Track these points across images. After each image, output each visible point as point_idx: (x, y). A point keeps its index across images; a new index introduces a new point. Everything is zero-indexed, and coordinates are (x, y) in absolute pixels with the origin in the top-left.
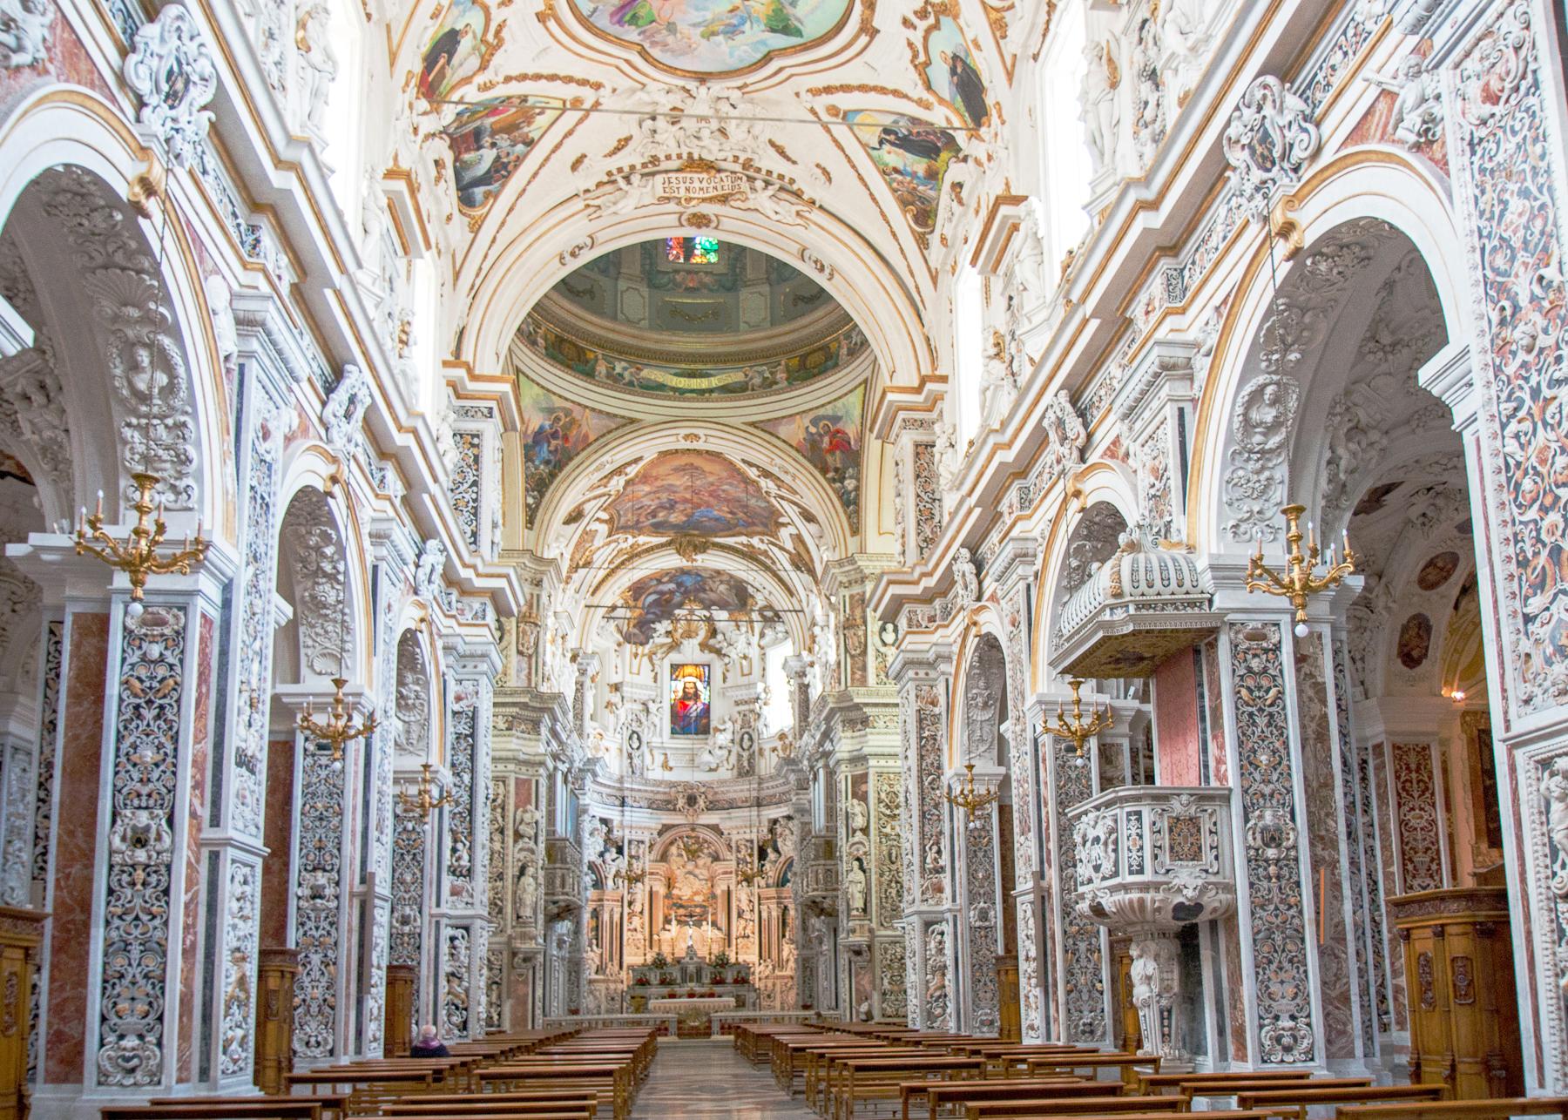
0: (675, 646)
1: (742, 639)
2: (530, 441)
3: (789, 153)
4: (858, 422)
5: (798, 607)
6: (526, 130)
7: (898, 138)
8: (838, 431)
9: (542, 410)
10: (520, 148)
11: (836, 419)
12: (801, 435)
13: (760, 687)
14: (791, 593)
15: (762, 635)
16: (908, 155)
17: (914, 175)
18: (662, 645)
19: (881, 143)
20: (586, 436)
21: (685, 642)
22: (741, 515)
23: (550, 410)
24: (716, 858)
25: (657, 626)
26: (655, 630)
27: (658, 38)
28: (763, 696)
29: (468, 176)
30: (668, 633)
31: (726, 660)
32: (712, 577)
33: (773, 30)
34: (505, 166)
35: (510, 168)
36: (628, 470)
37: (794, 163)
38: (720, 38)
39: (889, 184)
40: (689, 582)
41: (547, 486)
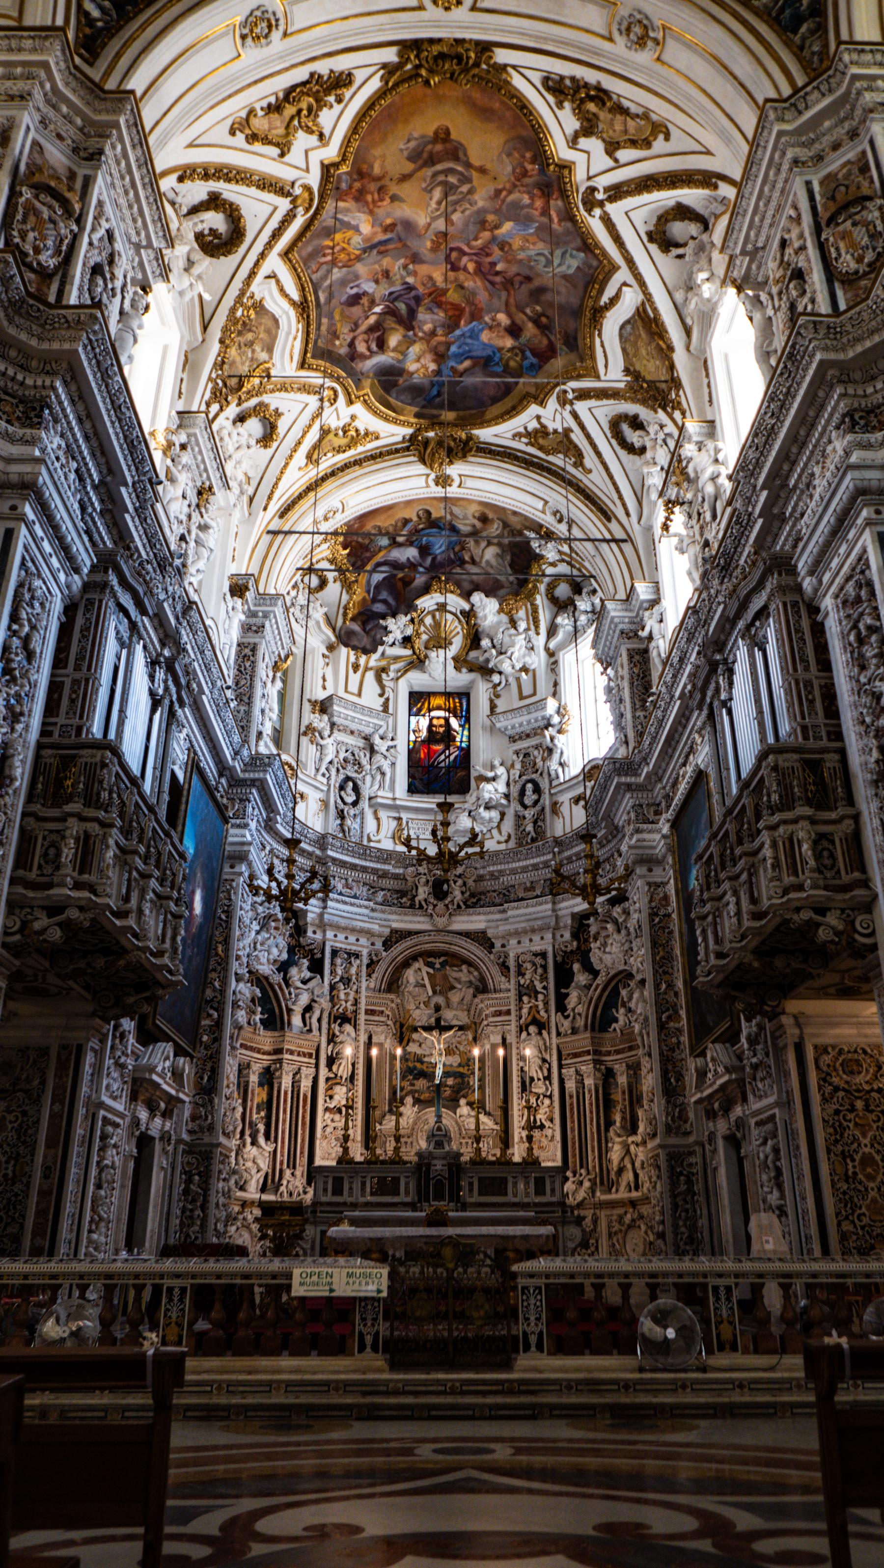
0: (418, 663)
1: (520, 641)
5: (620, 534)
13: (551, 705)
14: (606, 515)
15: (552, 631)
18: (396, 659)
21: (433, 654)
22: (530, 330)
24: (482, 988)
25: (390, 623)
26: (386, 631)
28: (556, 720)
30: (407, 641)
31: (496, 678)
32: (475, 533)
36: (326, 118)
40: (439, 545)
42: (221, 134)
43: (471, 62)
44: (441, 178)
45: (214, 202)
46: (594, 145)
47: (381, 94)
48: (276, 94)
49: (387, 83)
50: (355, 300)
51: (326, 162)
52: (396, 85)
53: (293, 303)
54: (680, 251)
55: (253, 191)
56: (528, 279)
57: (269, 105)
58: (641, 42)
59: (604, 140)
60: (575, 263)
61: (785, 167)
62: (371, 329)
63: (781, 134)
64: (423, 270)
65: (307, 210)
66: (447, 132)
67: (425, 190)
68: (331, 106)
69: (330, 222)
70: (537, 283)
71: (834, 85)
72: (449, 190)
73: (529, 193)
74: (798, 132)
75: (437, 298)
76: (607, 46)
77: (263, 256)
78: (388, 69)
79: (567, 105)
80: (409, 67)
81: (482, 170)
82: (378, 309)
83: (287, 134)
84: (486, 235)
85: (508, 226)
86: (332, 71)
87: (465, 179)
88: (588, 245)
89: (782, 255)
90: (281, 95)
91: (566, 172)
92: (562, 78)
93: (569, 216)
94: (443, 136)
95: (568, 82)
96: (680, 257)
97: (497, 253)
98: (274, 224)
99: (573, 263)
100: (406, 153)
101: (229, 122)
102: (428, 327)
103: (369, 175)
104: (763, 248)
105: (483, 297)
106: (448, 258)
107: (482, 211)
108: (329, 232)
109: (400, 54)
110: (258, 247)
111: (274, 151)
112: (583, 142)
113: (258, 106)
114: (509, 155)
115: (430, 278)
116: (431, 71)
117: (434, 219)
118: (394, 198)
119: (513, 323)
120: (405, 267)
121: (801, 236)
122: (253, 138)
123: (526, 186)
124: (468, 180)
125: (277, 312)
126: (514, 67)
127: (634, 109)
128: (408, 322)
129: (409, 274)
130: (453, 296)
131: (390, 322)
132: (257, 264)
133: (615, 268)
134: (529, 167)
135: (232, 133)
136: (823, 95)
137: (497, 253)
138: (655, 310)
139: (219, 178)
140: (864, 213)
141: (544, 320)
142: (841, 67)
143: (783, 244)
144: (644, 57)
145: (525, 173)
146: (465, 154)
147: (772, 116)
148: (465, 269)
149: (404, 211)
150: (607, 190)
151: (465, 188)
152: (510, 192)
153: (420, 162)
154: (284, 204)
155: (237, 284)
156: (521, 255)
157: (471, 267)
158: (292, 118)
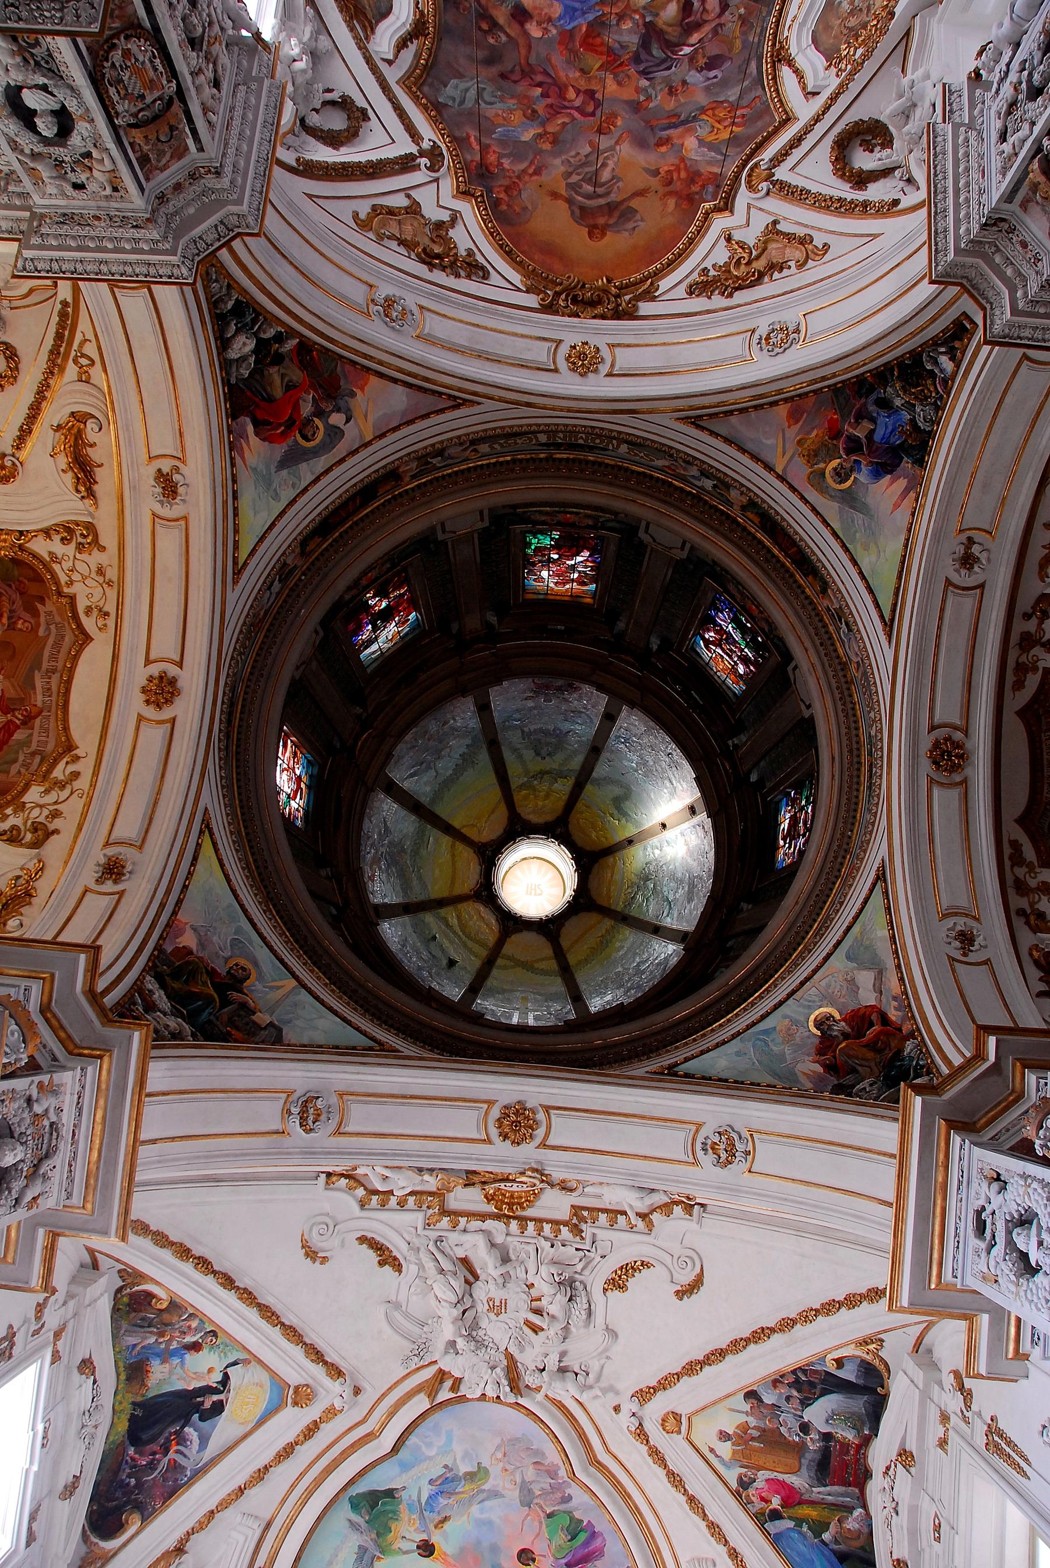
2: (907, 464)
3: (372, 1256)
4: (243, 475)
6: (752, 1421)
7: (197, 1408)
8: (284, 436)
9: (863, 508)
10: (769, 1398)
11: (291, 460)
12: (360, 401)
16: (179, 1386)
17: (165, 1356)
19: (226, 1379)
20: (794, 416)
23: (850, 499)
27: (546, 1482)
29: (858, 1404)
33: (390, 1493)
34: (797, 1384)
35: (791, 1379)
36: (721, 255)
37: (362, 1240)
38: (463, 1468)
39: (203, 1318)
41: (900, 361)
42: (838, 246)
43: (563, 296)
44: (600, 191)
45: (861, 180)
46: (432, 213)
47: (659, 274)
48: (771, 280)
49: (652, 284)
50: (713, 63)
51: (727, 213)
52: (643, 281)
53: (790, 63)
54: (329, 96)
55: (814, 188)
56: (503, 76)
57: (781, 270)
58: (389, 303)
59: (423, 217)
60: (449, 90)
61: (228, 170)
62: (698, 26)
63: (239, 202)
64: (627, 94)
65: (756, 165)
66: (591, 235)
67: (619, 180)
68: (714, 266)
69: (731, 151)
70: (494, 70)
71: (191, 246)
72: (594, 179)
73: (503, 169)
74: (222, 204)
75: (613, 62)
76: (425, 303)
77: (817, 119)
78: (650, 296)
79: (464, 254)
80: (627, 297)
81: (555, 195)
82: (687, 50)
83: (766, 242)
84: (551, 128)
85: (527, 136)
86: (709, 298)
87: (573, 187)
88: (436, 111)
89: (215, 71)
90: (766, 279)
91: (462, 188)
92: (469, 277)
93: (458, 142)
94: (596, 231)
95: (463, 273)
96: (329, 91)
97: (540, 107)
98: (797, 154)
99: (452, 91)
100: (638, 217)
101: (827, 257)
102: (627, 25)
103: (680, 197)
104: (237, 85)
105: (558, 59)
106: (598, 104)
107: (555, 154)
108: (734, 141)
109: (636, 308)
110: (820, 129)
111: (782, 227)
112: (445, 216)
113: (793, 269)
114: (525, 209)
115: (619, 84)
116: (606, 291)
117: (612, 149)
118: (656, 173)
119: (522, 24)
120: (649, 98)
121: (198, 89)
122: (805, 241)
123: (505, 177)
124: (569, 186)
125: (812, 52)
126: (519, 290)
127: (393, 245)
128: (651, 33)
129: (645, 90)
130: (594, 62)
131: (673, 34)
132: (826, 109)
133: (402, 82)
134: (502, 195)
135: (826, 247)
136: (200, 238)
137: (540, 107)
138: (352, 29)
139: (852, 202)
140: (134, 110)
141: (485, 27)
142: (188, 263)
143: (217, 84)
144: (385, 290)
145: (507, 189)
146: (573, 213)
147: (250, 220)
148: (578, 92)
149: (644, 159)
150: (418, 167)
151: (575, 178)
152: (524, 171)
153: (623, 207)
154: (782, 173)
155: (854, 88)
156: (512, 103)
157: (571, 94)
158: (758, 257)
